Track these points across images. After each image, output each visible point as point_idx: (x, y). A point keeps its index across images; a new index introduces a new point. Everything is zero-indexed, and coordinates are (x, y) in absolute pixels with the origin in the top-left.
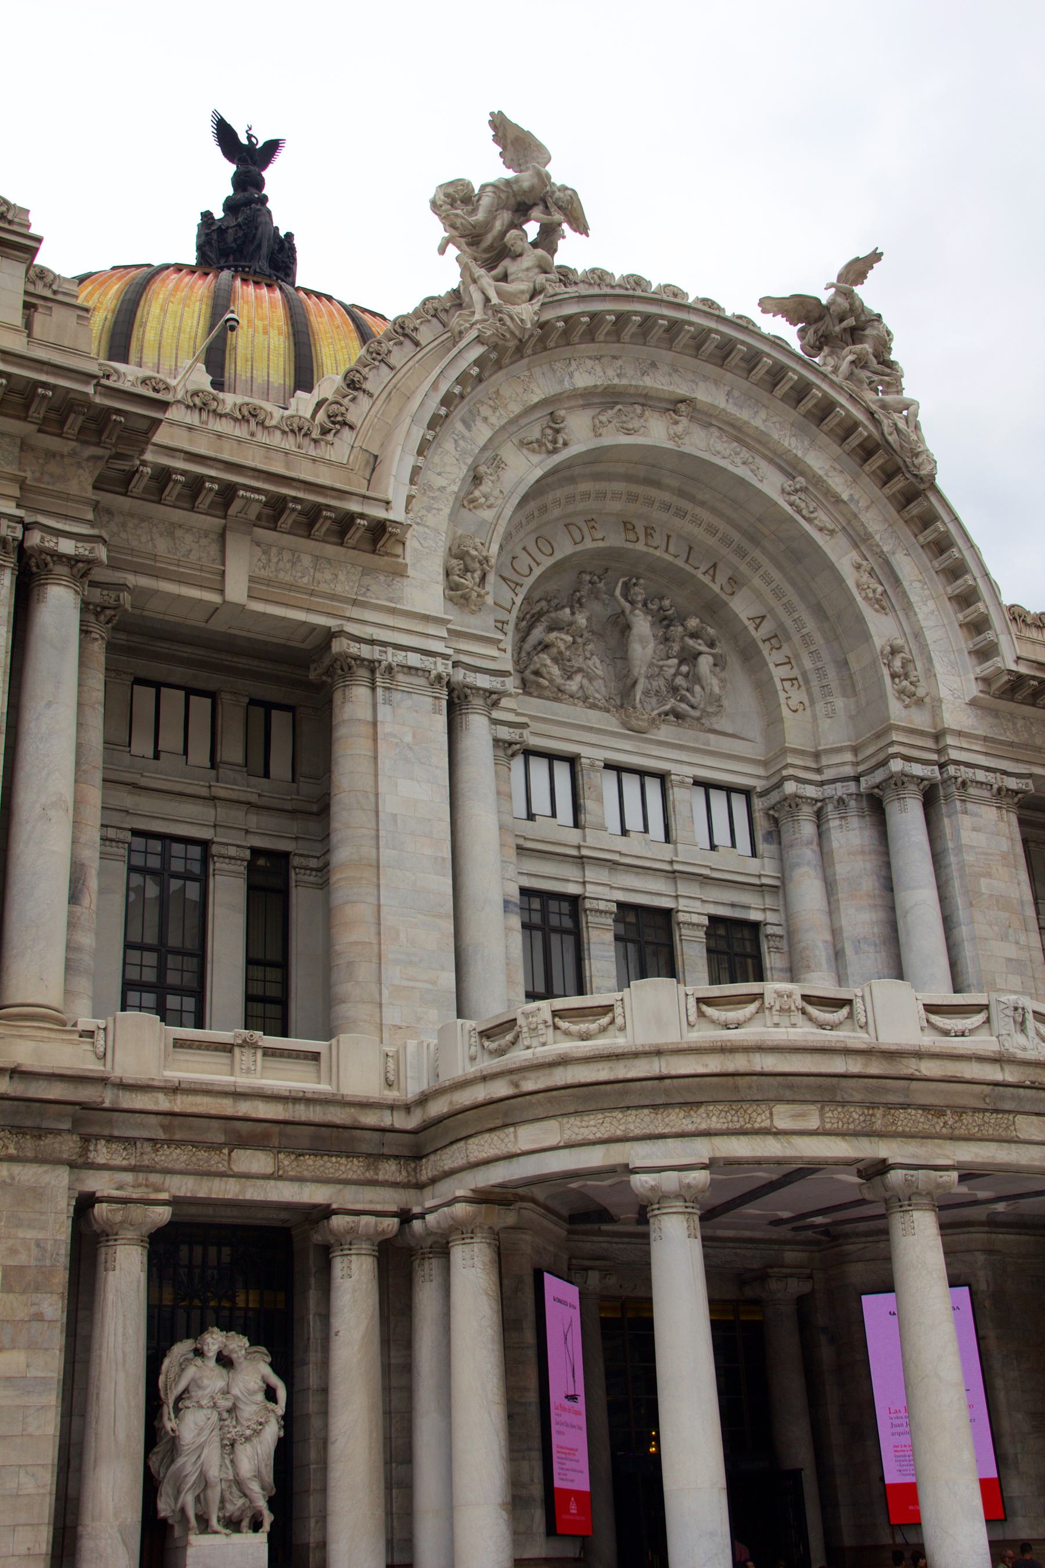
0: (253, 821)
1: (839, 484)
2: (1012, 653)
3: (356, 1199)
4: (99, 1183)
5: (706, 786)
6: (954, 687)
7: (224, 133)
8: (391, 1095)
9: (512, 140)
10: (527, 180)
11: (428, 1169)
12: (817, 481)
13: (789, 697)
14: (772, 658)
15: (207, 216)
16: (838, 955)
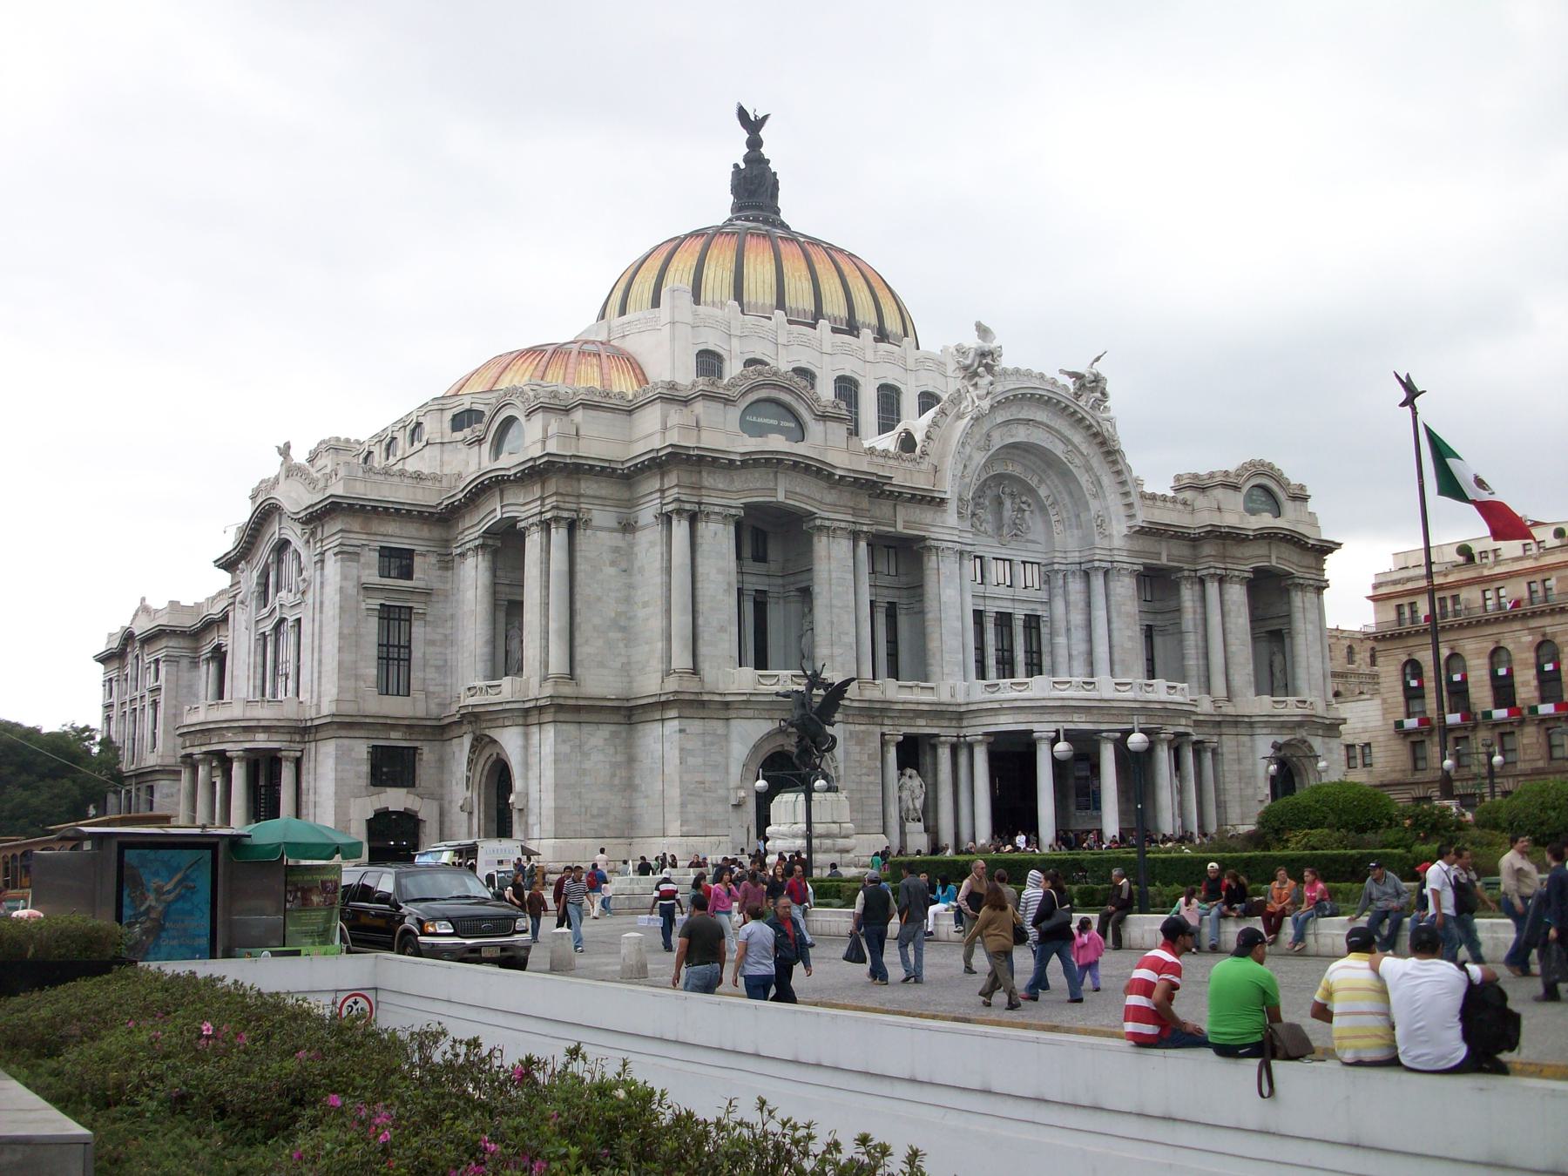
0: (886, 592)
1: (1084, 448)
2: (1141, 518)
3: (946, 732)
4: (886, 730)
5: (1024, 563)
6: (1119, 528)
7: (742, 114)
8: (953, 701)
9: (983, 331)
10: (987, 346)
11: (965, 723)
12: (1076, 447)
13: (1057, 528)
14: (1052, 512)
15: (736, 166)
16: (1068, 630)
